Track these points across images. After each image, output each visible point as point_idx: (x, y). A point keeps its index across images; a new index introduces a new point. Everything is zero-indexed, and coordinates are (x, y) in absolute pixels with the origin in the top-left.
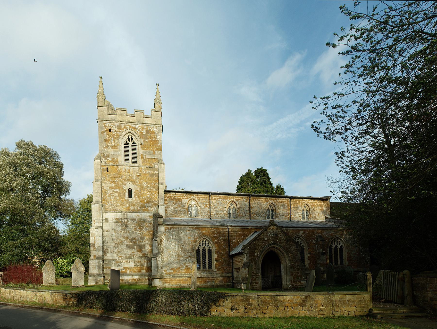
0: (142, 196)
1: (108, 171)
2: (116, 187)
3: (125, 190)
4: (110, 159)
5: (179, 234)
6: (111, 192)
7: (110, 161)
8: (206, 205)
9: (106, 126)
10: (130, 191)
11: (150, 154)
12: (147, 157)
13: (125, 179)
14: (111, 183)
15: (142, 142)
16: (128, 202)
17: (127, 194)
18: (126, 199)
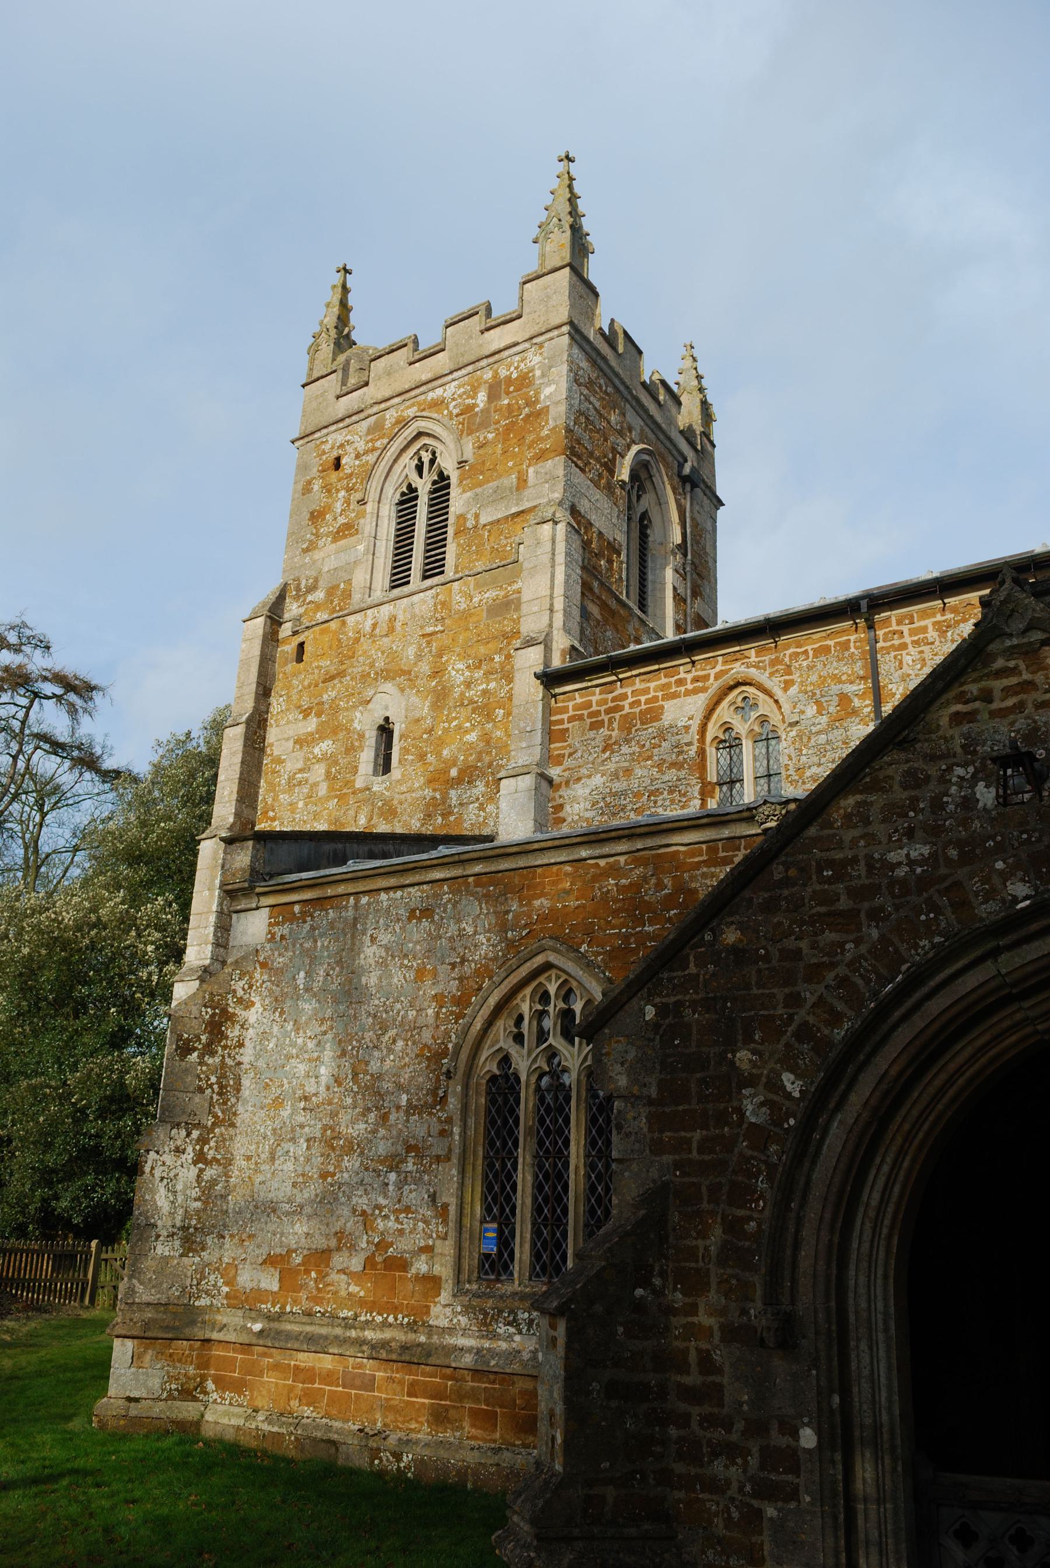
0: (441, 743)
1: (299, 659)
2: (321, 734)
3: (361, 736)
4: (319, 595)
5: (354, 950)
6: (300, 765)
7: (318, 606)
8: (844, 699)
9: (324, 453)
10: (385, 731)
11: (499, 495)
12: (483, 520)
13: (364, 676)
14: (306, 713)
15: (469, 453)
16: (365, 801)
17: (367, 757)
18: (359, 784)
